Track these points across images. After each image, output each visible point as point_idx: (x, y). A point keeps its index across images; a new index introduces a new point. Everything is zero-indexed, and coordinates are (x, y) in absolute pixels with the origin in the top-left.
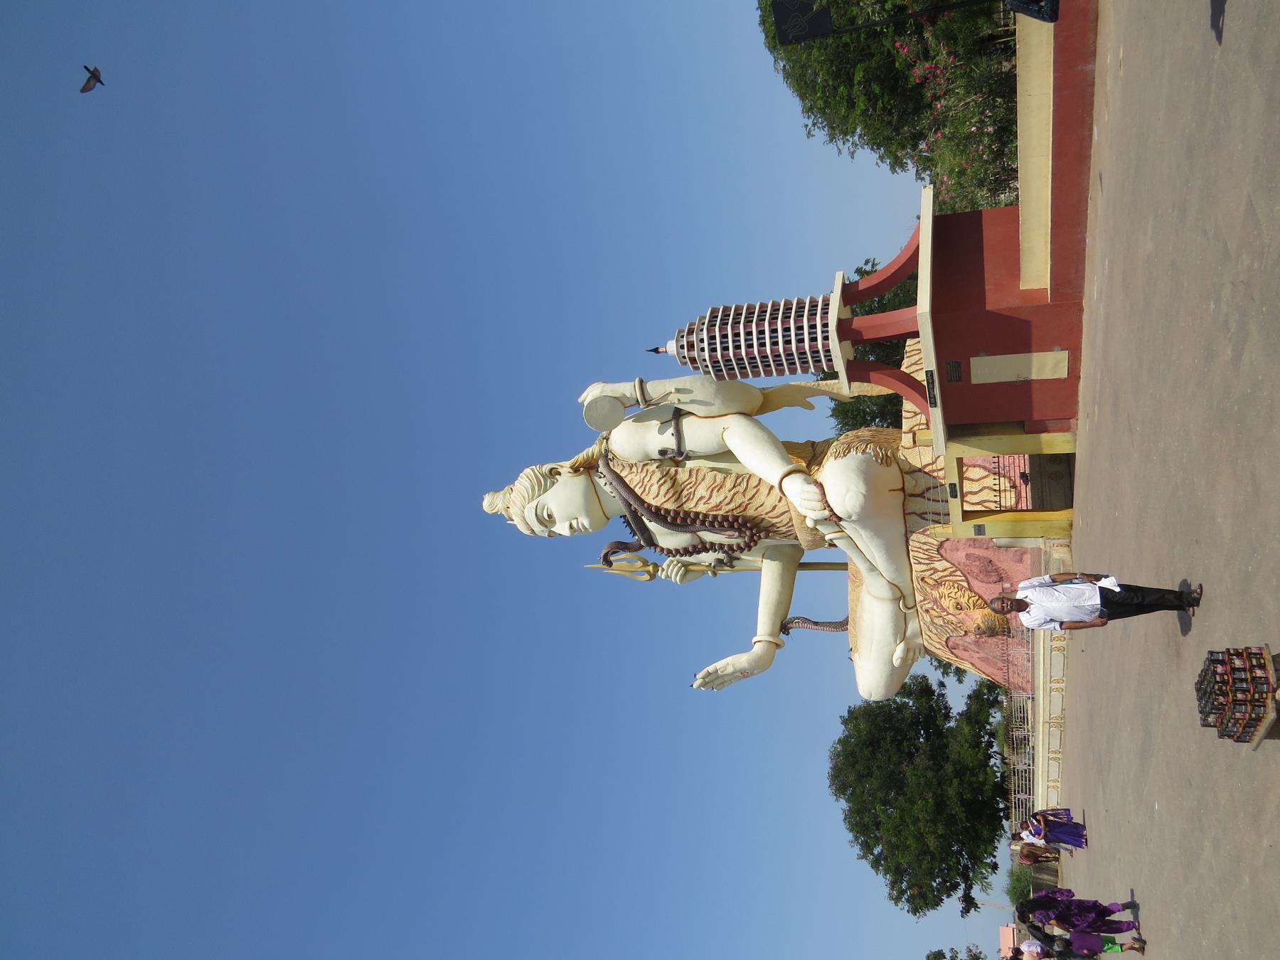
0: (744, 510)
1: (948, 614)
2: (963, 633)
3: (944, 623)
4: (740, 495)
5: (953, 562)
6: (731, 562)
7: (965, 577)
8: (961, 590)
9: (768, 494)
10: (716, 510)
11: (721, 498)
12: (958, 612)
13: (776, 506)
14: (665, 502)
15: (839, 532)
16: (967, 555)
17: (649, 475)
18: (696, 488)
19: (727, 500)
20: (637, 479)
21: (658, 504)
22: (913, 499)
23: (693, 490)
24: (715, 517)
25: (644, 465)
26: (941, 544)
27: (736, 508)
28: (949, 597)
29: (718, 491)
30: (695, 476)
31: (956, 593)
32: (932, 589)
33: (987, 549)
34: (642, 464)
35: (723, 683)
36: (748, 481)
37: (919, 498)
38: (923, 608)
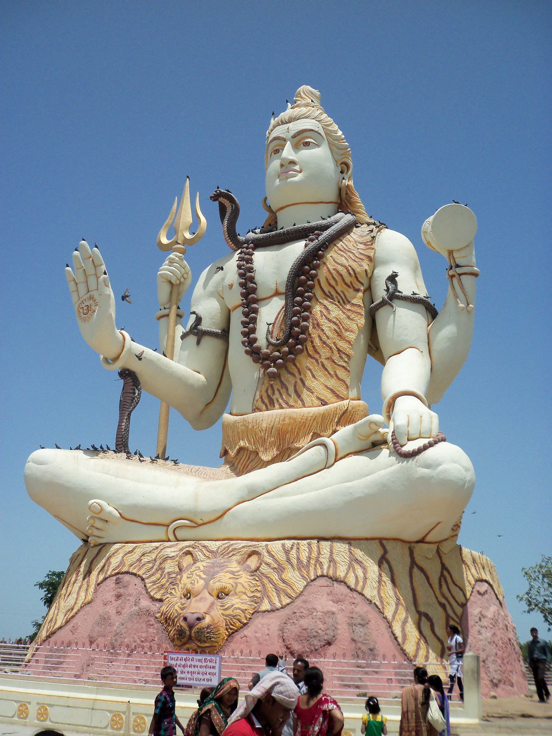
0: (310, 356)
2: (158, 596)
4: (328, 355)
5: (305, 593)
6: (195, 334)
7: (282, 608)
9: (326, 386)
12: (215, 593)
13: (312, 393)
15: (336, 455)
17: (357, 260)
19: (324, 338)
20: (350, 245)
22: (407, 552)
25: (370, 259)
27: (314, 347)
28: (236, 583)
29: (335, 330)
31: (245, 593)
33: (354, 640)
36: (343, 367)
37: (408, 560)
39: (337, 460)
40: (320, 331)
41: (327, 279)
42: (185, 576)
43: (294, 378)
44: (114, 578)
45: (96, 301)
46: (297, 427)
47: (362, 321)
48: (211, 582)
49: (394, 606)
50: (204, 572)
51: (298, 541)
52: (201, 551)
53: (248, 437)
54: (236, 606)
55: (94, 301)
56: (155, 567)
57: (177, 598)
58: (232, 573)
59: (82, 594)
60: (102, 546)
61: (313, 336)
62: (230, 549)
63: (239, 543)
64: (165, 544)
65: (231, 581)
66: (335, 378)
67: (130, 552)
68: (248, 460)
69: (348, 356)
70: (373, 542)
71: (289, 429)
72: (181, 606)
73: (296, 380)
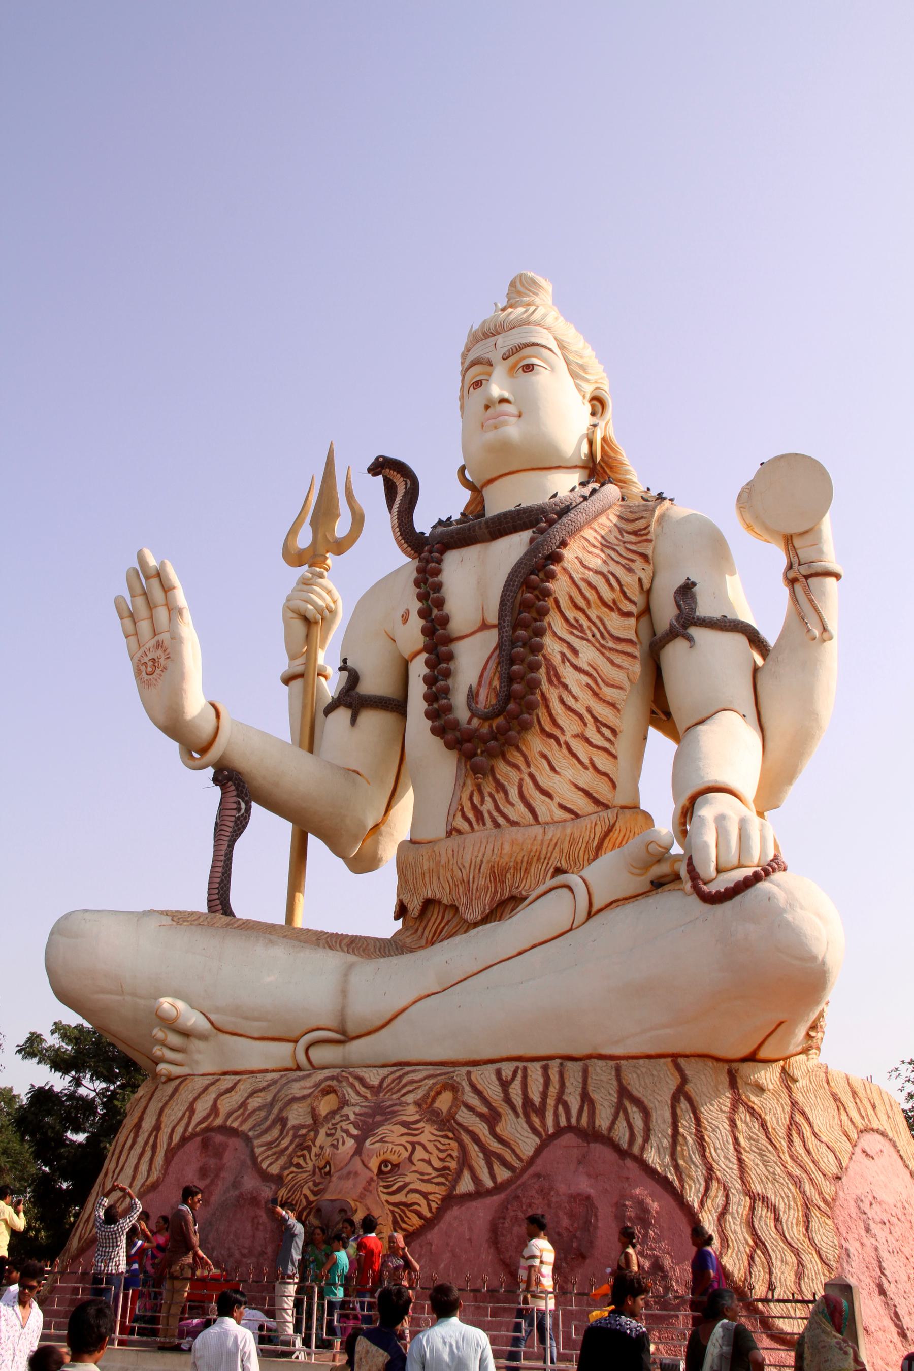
1: (360, 1141)
2: (274, 1170)
3: (296, 1128)
5: (539, 1161)
6: (349, 706)
8: (442, 1176)
10: (548, 674)
11: (575, 689)
12: (374, 1164)
14: (571, 578)
16: (588, 1198)
17: (623, 561)
18: (594, 646)
19: (570, 702)
21: (565, 564)
23: (590, 637)
24: (534, 667)
26: (591, 1135)
27: (551, 715)
28: (413, 1144)
29: (588, 685)
30: (619, 647)
31: (429, 1162)
32: (418, 1104)
34: (649, 552)
35: (131, 616)
36: (605, 750)
38: (334, 1083)
39: (592, 913)
40: (561, 689)
41: (571, 598)
42: (323, 1132)
43: (518, 773)
44: (199, 1139)
45: (167, 652)
46: (525, 859)
47: (636, 668)
48: (368, 1142)
49: (703, 1183)
50: (356, 1126)
51: (525, 1064)
52: (353, 1086)
53: (439, 879)
54: (411, 1186)
55: (165, 651)
56: (272, 1117)
57: (308, 1174)
58: (405, 1124)
59: (144, 1167)
60: (178, 1081)
61: (548, 696)
62: (404, 1081)
63: (419, 1070)
64: (289, 1076)
65: (403, 1140)
66: (591, 769)
67: (229, 1090)
68: (440, 924)
69: (614, 732)
70: (662, 1060)
71: (512, 864)
72: (312, 1187)
73: (522, 776)
